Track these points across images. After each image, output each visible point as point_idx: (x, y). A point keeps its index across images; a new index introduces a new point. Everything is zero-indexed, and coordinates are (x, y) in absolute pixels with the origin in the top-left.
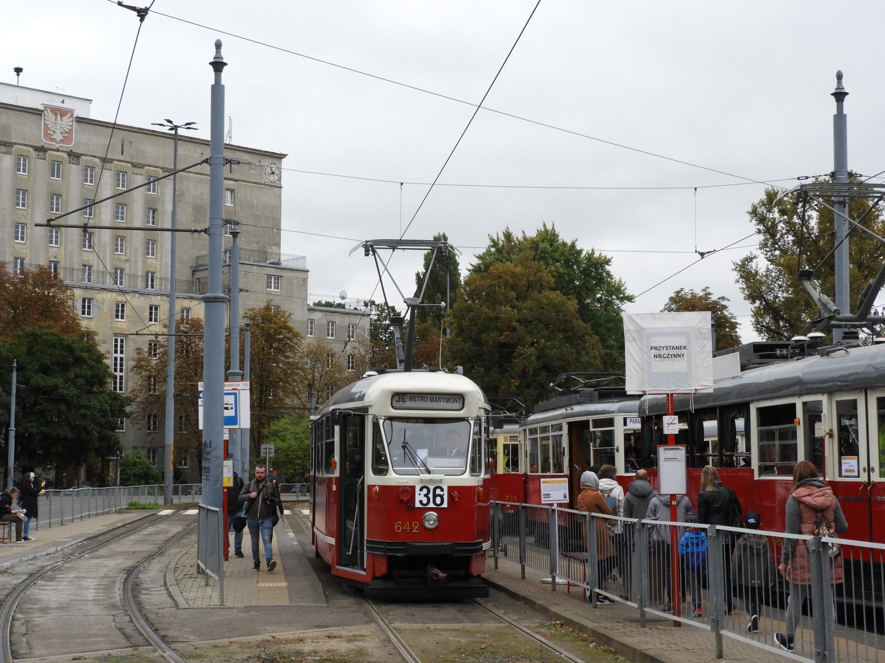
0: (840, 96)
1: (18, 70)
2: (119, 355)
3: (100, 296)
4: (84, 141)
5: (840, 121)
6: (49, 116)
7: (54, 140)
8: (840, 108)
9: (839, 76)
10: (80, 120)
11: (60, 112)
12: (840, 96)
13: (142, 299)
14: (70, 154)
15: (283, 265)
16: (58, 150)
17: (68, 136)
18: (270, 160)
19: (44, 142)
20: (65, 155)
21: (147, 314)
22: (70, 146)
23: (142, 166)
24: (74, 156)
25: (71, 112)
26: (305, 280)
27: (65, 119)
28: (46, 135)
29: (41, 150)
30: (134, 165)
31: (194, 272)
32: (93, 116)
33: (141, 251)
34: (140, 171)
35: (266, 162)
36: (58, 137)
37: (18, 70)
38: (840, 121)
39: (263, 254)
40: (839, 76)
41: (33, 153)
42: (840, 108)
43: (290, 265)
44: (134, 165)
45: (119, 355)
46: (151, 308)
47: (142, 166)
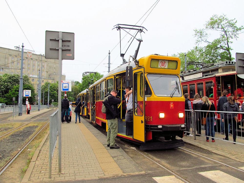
0: (109, 53)
2: (38, 87)
3: (35, 79)
4: (33, 57)
5: (109, 57)
8: (109, 55)
9: (109, 51)
10: (33, 54)
11: (30, 53)
12: (109, 53)
14: (31, 59)
19: (27, 57)
22: (31, 58)
24: (32, 59)
26: (65, 77)
27: (30, 54)
28: (28, 56)
36: (29, 56)
38: (109, 57)
40: (109, 51)
41: (26, 59)
42: (109, 55)
43: (63, 75)
45: (38, 87)
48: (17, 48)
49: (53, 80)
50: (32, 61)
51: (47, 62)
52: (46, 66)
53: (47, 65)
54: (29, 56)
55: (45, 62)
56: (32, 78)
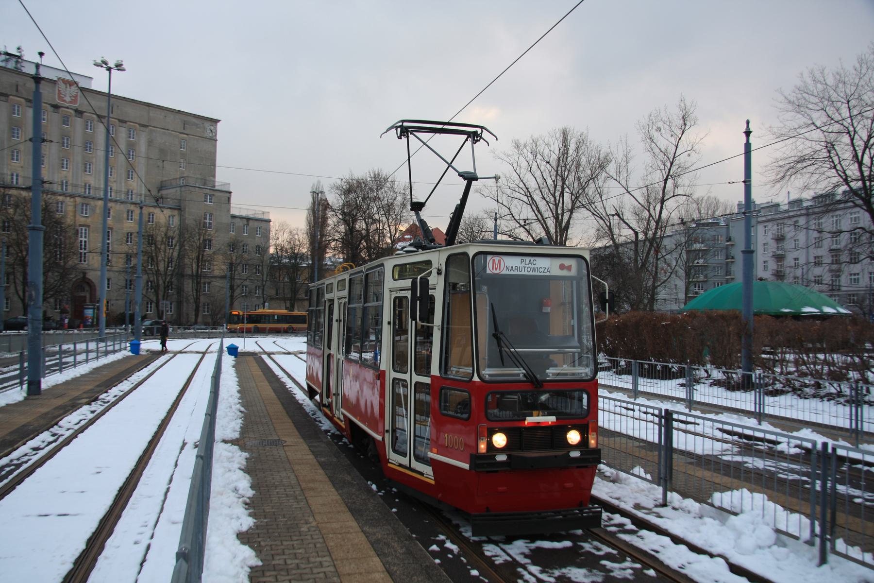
1: (41, 54)
3: (92, 203)
6: (62, 86)
7: (64, 101)
10: (83, 90)
13: (122, 206)
14: (76, 111)
15: (216, 188)
16: (67, 108)
17: (74, 101)
18: (210, 123)
19: (58, 101)
20: (72, 112)
21: (125, 216)
23: (125, 122)
24: (79, 113)
25: (76, 83)
26: (229, 199)
28: (60, 97)
29: (56, 107)
30: (120, 121)
31: (159, 191)
32: (93, 88)
33: (124, 175)
34: (124, 125)
35: (207, 125)
36: (68, 99)
37: (41, 54)
39: (205, 182)
44: (120, 121)
46: (128, 212)
47: (125, 122)
48: (7, 61)
49: (176, 212)
50: (79, 121)
51: (147, 130)
52: (142, 148)
53: (150, 143)
54: (68, 99)
55: (142, 128)
56: (78, 200)
